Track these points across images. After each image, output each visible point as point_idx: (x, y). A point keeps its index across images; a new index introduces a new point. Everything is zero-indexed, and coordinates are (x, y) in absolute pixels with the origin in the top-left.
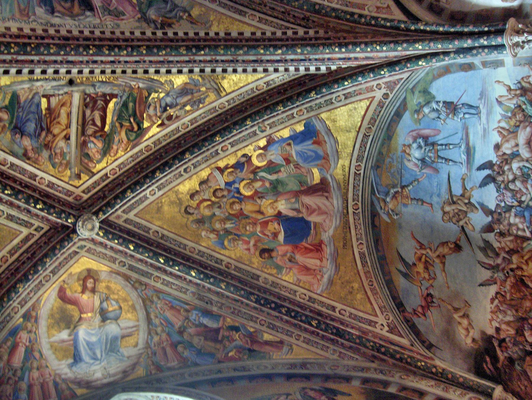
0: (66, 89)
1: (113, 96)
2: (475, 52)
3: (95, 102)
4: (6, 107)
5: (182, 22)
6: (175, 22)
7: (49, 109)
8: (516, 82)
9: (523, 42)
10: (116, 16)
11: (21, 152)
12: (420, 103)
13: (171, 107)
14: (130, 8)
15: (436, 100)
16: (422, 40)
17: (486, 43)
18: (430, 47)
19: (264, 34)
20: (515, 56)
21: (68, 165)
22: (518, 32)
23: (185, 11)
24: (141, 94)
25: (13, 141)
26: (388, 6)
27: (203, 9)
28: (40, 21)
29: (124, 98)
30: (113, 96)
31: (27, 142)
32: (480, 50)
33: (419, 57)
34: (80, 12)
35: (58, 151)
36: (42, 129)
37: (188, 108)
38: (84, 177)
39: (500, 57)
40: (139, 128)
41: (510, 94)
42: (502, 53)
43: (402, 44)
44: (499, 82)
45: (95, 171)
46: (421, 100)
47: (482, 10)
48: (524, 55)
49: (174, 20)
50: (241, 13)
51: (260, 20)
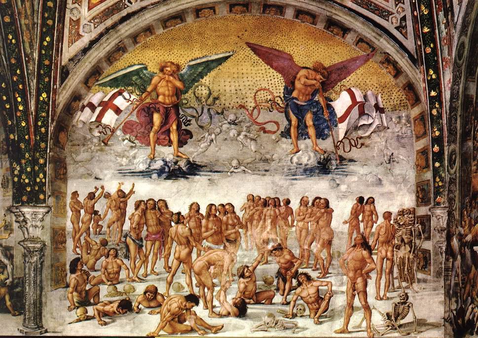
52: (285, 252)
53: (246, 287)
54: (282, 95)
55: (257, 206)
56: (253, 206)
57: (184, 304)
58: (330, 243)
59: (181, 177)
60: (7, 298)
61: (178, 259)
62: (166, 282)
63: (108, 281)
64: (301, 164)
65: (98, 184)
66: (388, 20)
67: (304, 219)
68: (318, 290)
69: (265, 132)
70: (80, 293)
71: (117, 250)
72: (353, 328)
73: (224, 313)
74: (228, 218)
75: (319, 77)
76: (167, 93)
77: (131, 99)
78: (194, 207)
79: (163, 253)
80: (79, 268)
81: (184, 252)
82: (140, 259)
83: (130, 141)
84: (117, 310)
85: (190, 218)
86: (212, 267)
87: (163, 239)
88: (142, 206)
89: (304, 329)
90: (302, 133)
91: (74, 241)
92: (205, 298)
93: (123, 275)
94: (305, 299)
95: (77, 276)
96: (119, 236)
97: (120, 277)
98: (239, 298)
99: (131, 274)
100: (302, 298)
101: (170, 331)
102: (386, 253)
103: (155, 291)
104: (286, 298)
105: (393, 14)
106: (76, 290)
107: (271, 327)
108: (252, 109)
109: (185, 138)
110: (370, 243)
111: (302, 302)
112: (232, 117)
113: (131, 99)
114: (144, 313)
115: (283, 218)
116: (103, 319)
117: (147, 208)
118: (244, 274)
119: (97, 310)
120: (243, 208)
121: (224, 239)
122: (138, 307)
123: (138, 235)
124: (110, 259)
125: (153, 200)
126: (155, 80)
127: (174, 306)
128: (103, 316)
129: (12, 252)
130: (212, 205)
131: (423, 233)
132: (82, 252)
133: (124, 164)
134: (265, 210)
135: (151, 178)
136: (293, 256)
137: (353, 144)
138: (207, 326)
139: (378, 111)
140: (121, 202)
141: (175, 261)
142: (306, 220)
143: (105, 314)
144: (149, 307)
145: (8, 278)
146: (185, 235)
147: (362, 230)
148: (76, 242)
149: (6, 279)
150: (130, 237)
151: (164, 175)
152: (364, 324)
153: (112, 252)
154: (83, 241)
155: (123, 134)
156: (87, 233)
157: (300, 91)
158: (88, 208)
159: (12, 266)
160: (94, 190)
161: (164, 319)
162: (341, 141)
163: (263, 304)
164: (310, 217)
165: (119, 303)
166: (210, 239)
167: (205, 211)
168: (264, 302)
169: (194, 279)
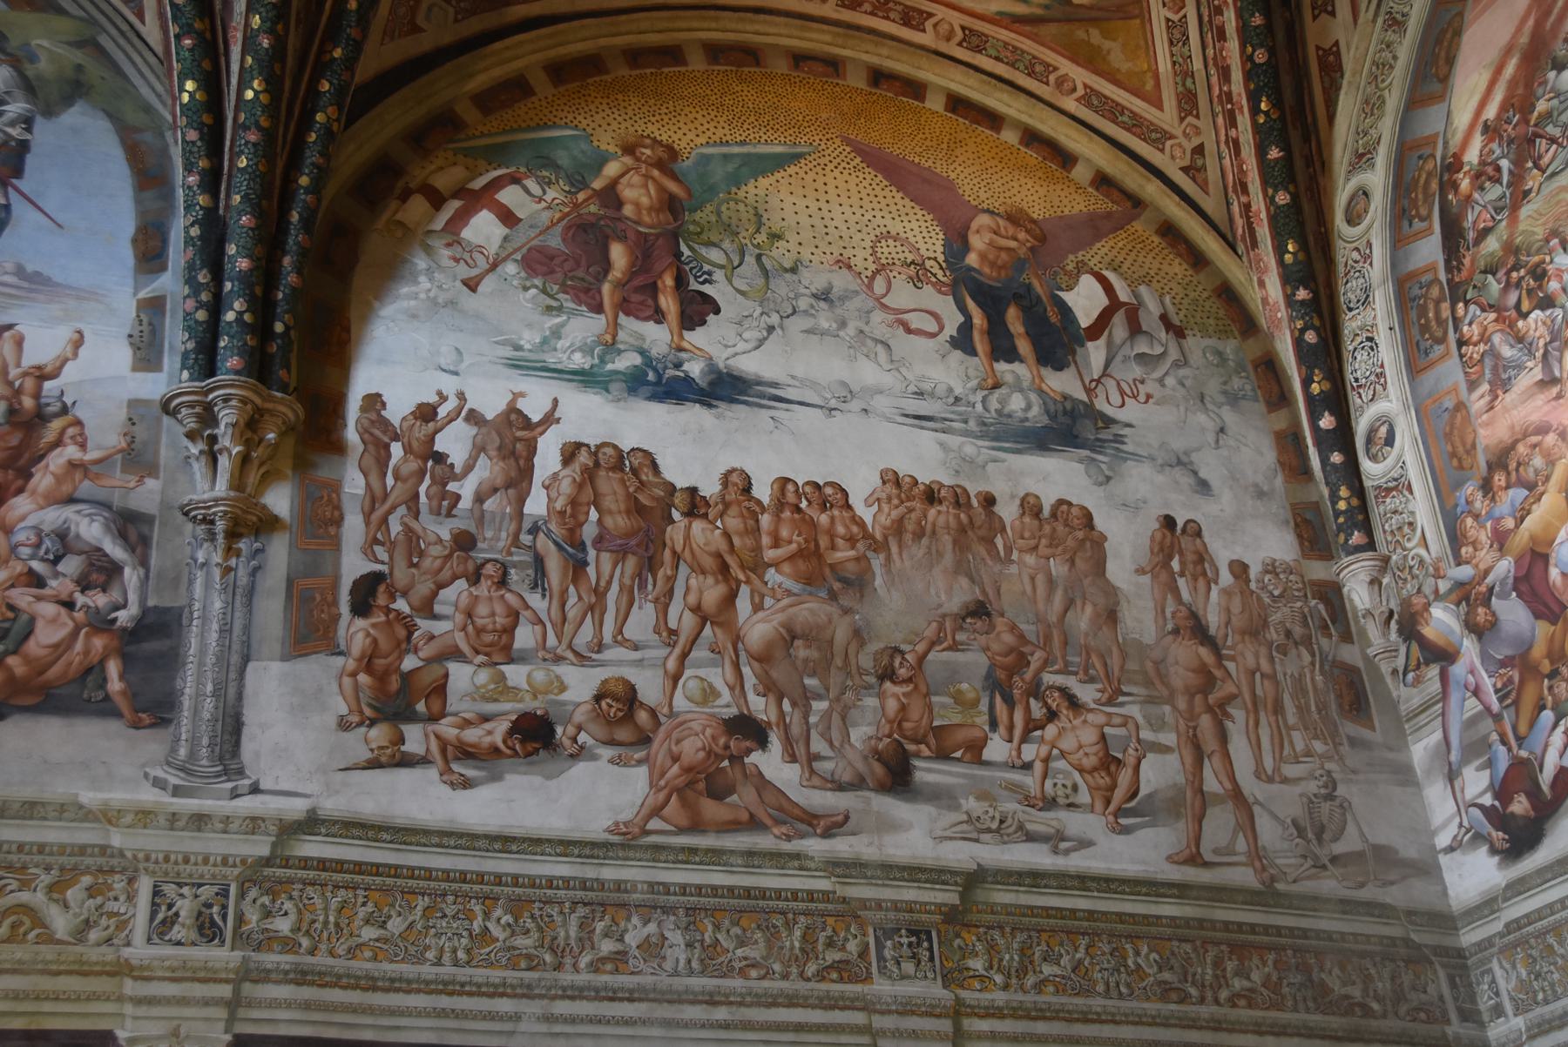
2: (203, 277)
8: (68, 400)
9: (213, 440)
12: (33, 59)
15: (39, 121)
16: (272, 109)
17: (230, 316)
18: (245, 128)
20: (167, 407)
22: (250, 427)
26: (416, 29)
32: (204, 297)
33: (213, 84)
39: (170, 361)
41: (25, 374)
42: (183, 367)
43: (271, 32)
44: (78, 342)
46: (44, 66)
47: (348, 330)
48: (164, 439)
52: (1000, 623)
53: (903, 708)
54: (941, 258)
55: (909, 499)
56: (899, 497)
57: (722, 741)
58: (1111, 616)
59: (695, 401)
60: (113, 668)
61: (696, 609)
62: (661, 672)
63: (477, 652)
64: (1009, 416)
65: (449, 385)
66: (1162, 151)
67: (1036, 548)
68: (1103, 737)
69: (909, 331)
70: (381, 678)
71: (503, 565)
72: (1216, 851)
73: (847, 777)
74: (832, 518)
75: (1022, 235)
76: (645, 201)
77: (549, 197)
78: (734, 478)
79: (650, 587)
80: (381, 600)
81: (713, 594)
82: (580, 598)
83: (544, 291)
84: (505, 742)
85: (727, 505)
86: (798, 643)
87: (647, 549)
88: (583, 458)
89: (1084, 844)
90: (1003, 349)
91: (367, 523)
92: (786, 728)
93: (524, 637)
94: (1074, 758)
95: (374, 626)
96: (513, 527)
97: (517, 645)
98: (889, 736)
99: (552, 640)
100: (1063, 754)
101: (684, 822)
102: (1257, 656)
103: (629, 697)
104: (1019, 750)
105: (1172, 137)
106: (369, 668)
107: (989, 830)
108: (869, 273)
109: (697, 310)
110: (1212, 631)
111: (1061, 764)
112: (819, 284)
113: (549, 197)
114: (594, 758)
115: (982, 539)
116: (455, 767)
117: (597, 464)
118: (893, 672)
119: (437, 737)
120: (871, 500)
121: (827, 571)
122: (574, 740)
123: (572, 531)
124: (483, 589)
125: (615, 447)
126: (612, 169)
127: (691, 749)
128: (457, 759)
129: (145, 529)
130: (787, 480)
131: (1334, 623)
132: (391, 558)
133: (527, 346)
134: (932, 512)
135: (607, 391)
136: (1022, 637)
137: (1128, 391)
138: (796, 811)
139: (1171, 334)
140: (520, 440)
141: (687, 614)
142: (1043, 550)
143: (467, 753)
144: (611, 742)
145: (124, 606)
146: (712, 548)
147: (1186, 595)
148: (373, 527)
149: (117, 608)
150: (548, 534)
151: (647, 390)
152: (1241, 844)
153: (489, 569)
154: (395, 527)
155: (523, 274)
156: (409, 508)
157: (983, 257)
158: (415, 444)
159: (142, 571)
160: (433, 399)
161: (662, 783)
162: (1098, 381)
163: (958, 760)
164: (1050, 546)
165: (515, 723)
166: (786, 568)
167: (769, 492)
168: (958, 754)
169: (746, 671)
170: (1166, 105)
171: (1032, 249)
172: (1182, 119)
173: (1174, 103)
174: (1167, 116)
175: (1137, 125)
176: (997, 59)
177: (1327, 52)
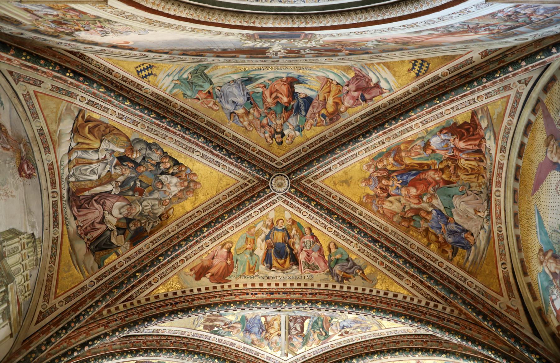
0: (276, 313)
1: (307, 317)
3: (296, 319)
4: (239, 322)
5: (356, 277)
6: (352, 277)
7: (266, 321)
10: (313, 270)
11: (250, 341)
13: (347, 327)
14: (322, 264)
19: (412, 299)
21: (280, 348)
23: (360, 269)
24: (326, 318)
25: (244, 336)
27: (373, 269)
28: (261, 275)
29: (315, 319)
30: (307, 317)
31: (253, 337)
34: (289, 266)
35: (273, 341)
36: (263, 331)
37: (359, 330)
38: (290, 356)
40: (326, 334)
45: (297, 353)
49: (351, 275)
50: (400, 276)
51: (413, 286)
75: (552, 143)
105: (518, 91)
170: (509, 94)
171: (556, 140)
172: (512, 89)
173: (507, 92)
174: (512, 93)
175: (517, 101)
176: (507, 142)
177: (482, 56)
